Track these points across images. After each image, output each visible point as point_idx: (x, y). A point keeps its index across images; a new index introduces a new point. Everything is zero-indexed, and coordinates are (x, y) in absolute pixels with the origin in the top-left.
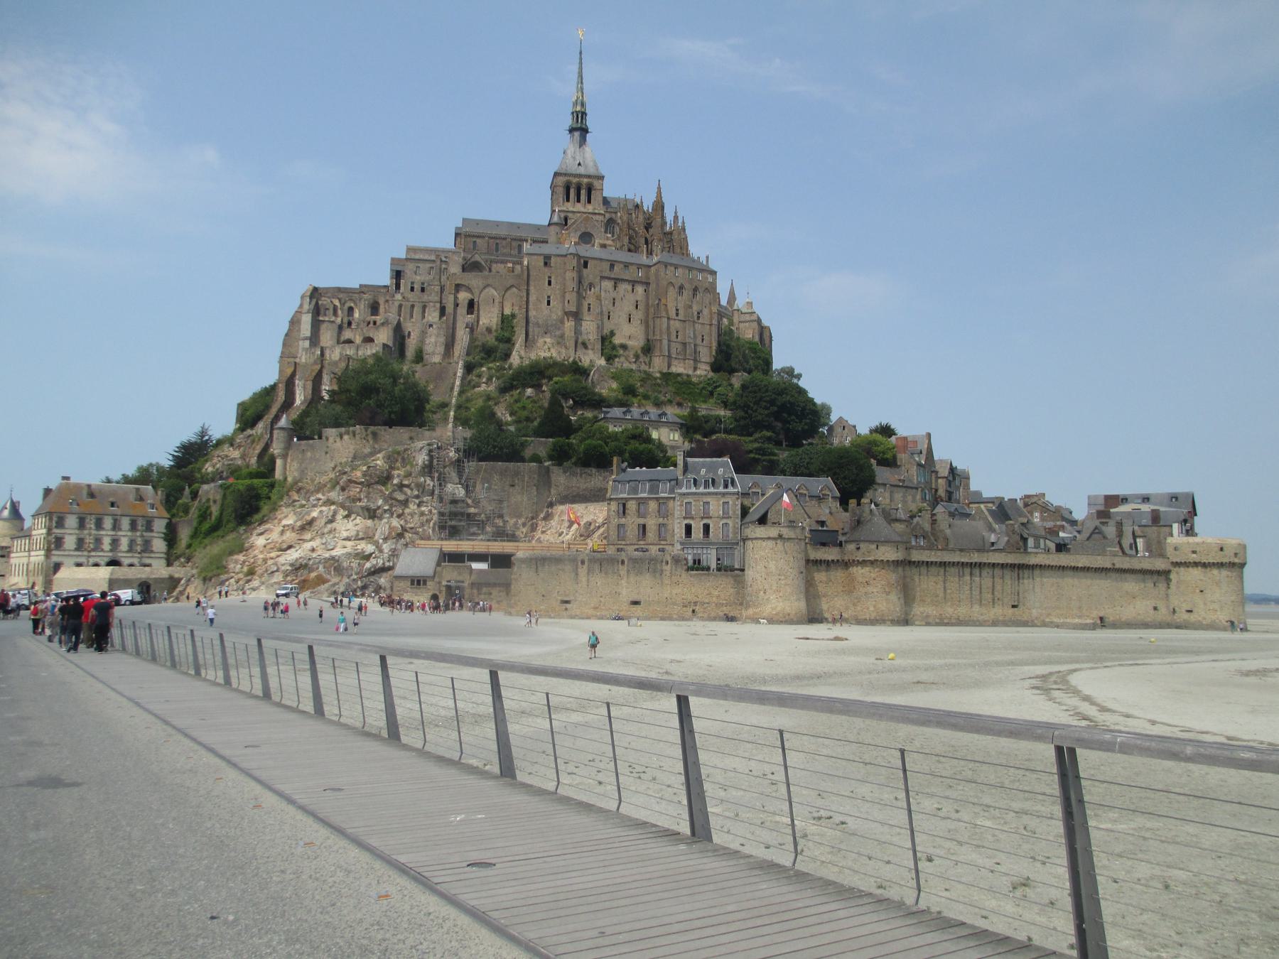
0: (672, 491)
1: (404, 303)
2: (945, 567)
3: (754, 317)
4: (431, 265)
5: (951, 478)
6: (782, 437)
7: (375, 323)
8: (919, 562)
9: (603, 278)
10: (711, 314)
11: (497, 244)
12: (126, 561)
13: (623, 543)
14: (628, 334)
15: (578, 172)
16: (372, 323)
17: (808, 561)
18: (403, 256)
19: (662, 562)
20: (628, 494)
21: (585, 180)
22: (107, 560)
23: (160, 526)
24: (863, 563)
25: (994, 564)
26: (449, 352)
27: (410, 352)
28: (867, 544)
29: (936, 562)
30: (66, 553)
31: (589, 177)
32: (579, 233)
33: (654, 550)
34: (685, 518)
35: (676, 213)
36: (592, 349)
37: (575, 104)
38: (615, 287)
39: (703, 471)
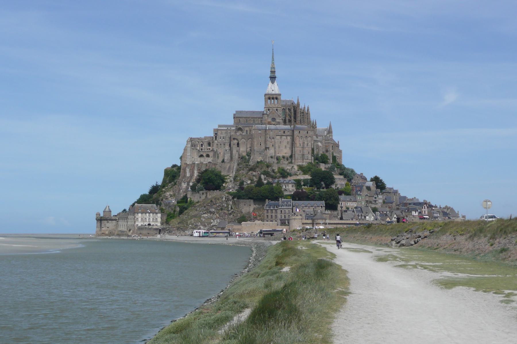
1: (218, 144)
4: (226, 131)
5: (376, 196)
6: (324, 186)
7: (209, 149)
9: (277, 135)
11: (247, 120)
12: (152, 224)
14: (285, 152)
18: (217, 127)
22: (148, 224)
23: (159, 215)
26: (232, 159)
31: (276, 95)
32: (271, 118)
34: (280, 214)
35: (305, 106)
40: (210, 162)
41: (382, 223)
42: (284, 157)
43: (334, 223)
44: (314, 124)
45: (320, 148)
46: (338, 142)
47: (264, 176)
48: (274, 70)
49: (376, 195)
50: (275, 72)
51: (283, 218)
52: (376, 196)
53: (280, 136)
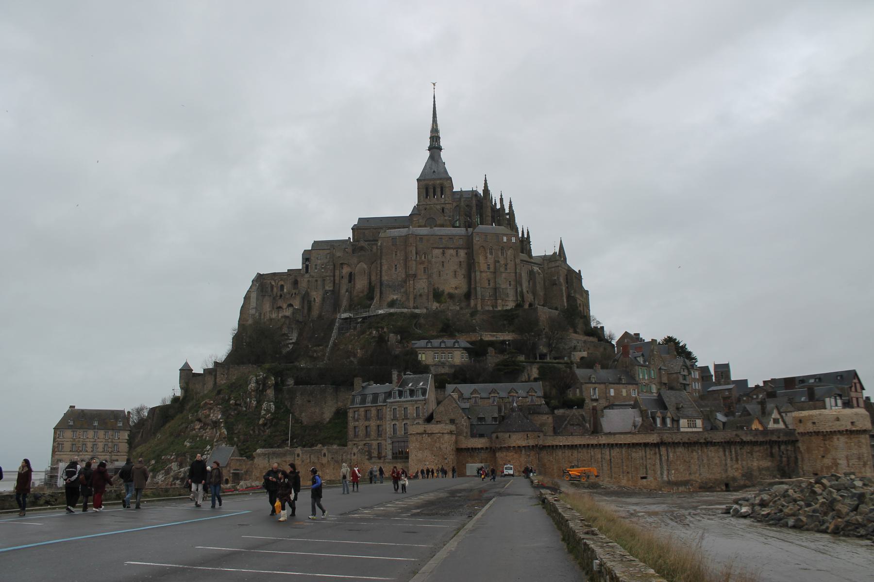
0: (385, 401)
1: (310, 279)
2: (578, 449)
3: (557, 264)
4: (328, 251)
5: (686, 373)
8: (553, 446)
10: (516, 265)
13: (357, 440)
14: (453, 286)
15: (432, 178)
16: (294, 294)
17: (459, 451)
19: (351, 454)
20: (360, 405)
21: (438, 182)
24: (501, 449)
25: (621, 444)
27: (315, 313)
28: (502, 434)
29: (568, 446)
30: (65, 453)
31: (441, 179)
33: (375, 443)
34: (392, 420)
35: (501, 196)
36: (428, 299)
37: (432, 131)
38: (443, 253)
39: (410, 385)
40: (286, 317)
41: (745, 439)
42: (451, 296)
43: (572, 445)
44: (526, 236)
45: (539, 279)
46: (580, 271)
47: (397, 336)
48: (436, 135)
49: (686, 371)
50: (440, 138)
51: (400, 432)
52: (686, 373)
53: (441, 250)
